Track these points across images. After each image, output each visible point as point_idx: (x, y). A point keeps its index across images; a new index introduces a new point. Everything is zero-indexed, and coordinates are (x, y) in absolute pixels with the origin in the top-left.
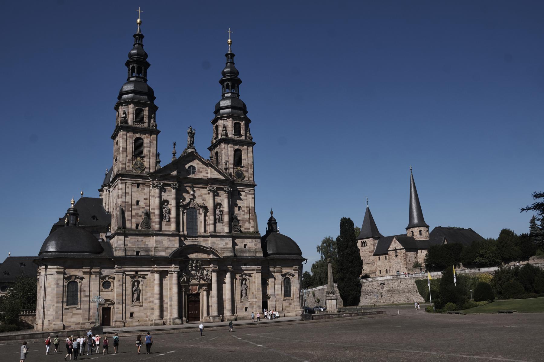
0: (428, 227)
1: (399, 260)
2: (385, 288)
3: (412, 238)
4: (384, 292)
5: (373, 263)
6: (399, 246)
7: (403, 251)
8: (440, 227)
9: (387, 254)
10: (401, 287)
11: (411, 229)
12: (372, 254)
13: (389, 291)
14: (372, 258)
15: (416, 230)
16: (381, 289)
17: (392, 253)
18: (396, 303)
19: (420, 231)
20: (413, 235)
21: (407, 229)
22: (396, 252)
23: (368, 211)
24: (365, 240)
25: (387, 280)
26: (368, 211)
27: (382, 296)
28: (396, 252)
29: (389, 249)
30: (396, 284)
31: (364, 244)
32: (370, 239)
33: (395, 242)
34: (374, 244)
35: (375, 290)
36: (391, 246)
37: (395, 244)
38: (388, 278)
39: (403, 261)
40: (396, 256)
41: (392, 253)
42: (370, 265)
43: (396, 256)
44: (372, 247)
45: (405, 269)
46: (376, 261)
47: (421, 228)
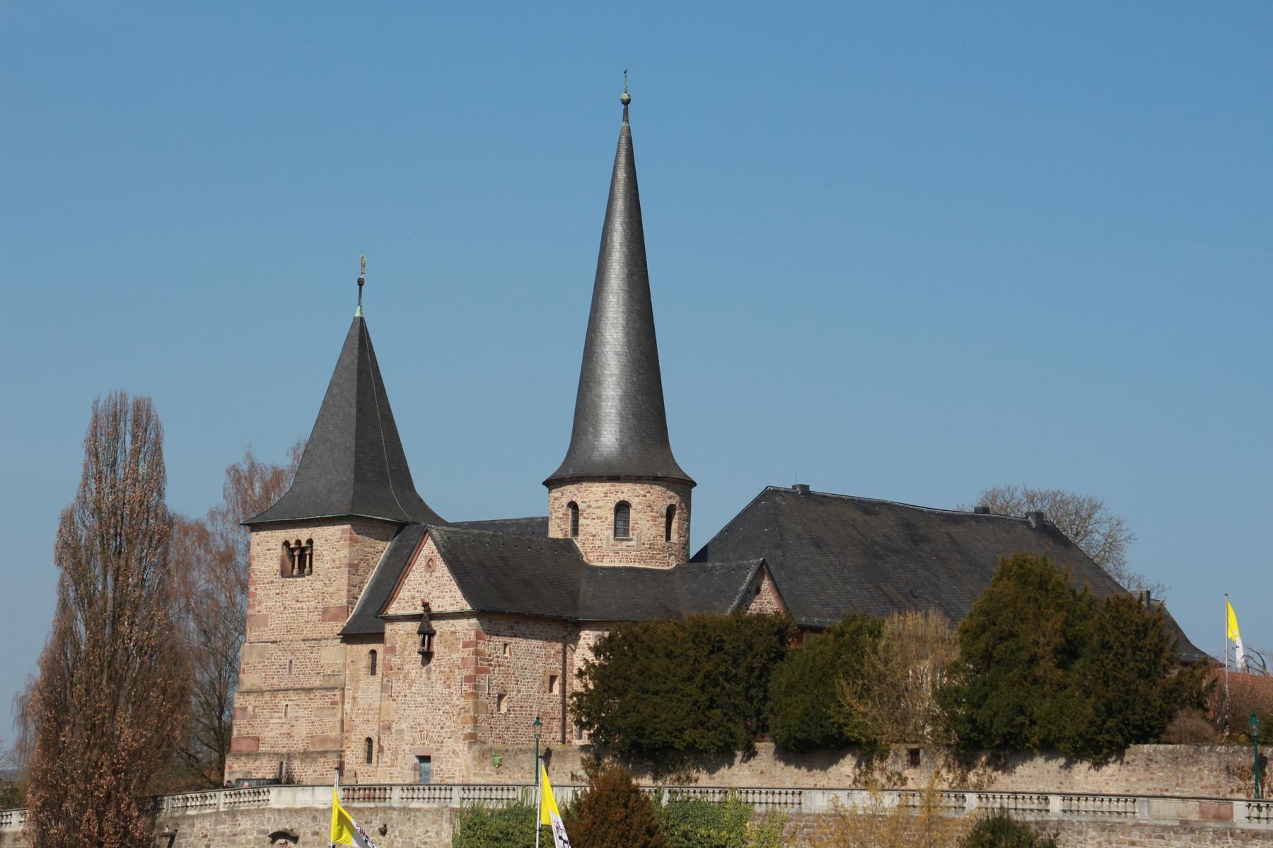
1: (439, 687)
3: (567, 547)
5: (334, 688)
6: (449, 596)
7: (467, 628)
9: (379, 637)
11: (570, 492)
12: (339, 627)
14: (335, 654)
17: (402, 635)
20: (575, 532)
21: (551, 484)
22: (427, 634)
24: (303, 534)
28: (427, 634)
29: (393, 610)
31: (299, 559)
32: (336, 532)
33: (430, 565)
34: (353, 568)
36: (405, 592)
37: (431, 583)
39: (458, 698)
40: (427, 656)
42: (318, 700)
43: (427, 656)
45: (462, 747)
46: (355, 679)
47: (626, 491)
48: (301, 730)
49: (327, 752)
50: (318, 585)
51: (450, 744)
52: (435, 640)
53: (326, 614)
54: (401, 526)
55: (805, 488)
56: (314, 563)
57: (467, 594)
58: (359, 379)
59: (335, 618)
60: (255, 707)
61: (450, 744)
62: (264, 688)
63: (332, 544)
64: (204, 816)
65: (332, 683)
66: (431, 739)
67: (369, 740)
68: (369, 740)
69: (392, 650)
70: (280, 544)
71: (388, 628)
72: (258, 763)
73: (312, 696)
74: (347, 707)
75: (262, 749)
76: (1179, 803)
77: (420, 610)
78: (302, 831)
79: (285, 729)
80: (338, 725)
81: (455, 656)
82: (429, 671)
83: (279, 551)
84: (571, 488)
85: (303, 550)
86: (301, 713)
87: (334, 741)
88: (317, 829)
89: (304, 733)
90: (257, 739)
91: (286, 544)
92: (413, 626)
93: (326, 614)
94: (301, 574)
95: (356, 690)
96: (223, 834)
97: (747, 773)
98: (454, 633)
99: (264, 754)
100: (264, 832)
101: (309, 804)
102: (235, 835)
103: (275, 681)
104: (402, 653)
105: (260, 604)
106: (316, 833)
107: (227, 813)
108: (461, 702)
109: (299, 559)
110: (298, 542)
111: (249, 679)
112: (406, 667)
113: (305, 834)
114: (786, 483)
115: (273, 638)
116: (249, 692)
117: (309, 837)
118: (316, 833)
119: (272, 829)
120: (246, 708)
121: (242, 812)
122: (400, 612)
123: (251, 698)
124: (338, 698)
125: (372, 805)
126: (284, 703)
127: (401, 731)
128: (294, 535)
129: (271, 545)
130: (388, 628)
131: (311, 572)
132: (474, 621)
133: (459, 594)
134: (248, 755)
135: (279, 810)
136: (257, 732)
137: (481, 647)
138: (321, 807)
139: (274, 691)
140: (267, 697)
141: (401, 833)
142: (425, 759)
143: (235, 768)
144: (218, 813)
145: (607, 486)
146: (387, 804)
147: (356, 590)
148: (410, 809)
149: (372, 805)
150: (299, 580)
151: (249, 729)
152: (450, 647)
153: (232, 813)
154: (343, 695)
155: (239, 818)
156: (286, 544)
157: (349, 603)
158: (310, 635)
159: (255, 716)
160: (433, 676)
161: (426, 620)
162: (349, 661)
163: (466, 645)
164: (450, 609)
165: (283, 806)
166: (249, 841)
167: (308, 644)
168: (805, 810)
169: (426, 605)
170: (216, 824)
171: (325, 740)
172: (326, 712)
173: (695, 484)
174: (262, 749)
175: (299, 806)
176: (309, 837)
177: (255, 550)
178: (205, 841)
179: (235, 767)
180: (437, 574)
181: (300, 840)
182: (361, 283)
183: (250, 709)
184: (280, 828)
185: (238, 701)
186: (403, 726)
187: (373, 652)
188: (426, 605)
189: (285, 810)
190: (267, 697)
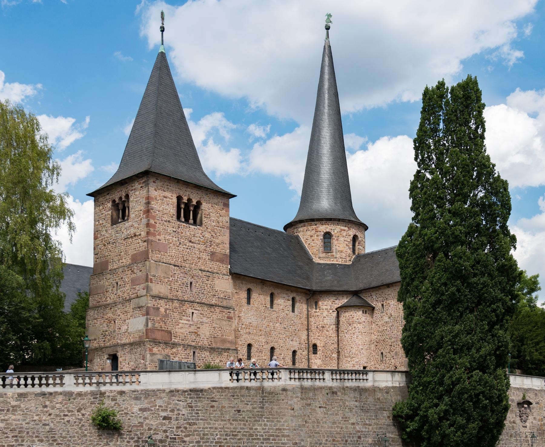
42: (217, 313)
48: (206, 331)
49: (229, 349)
50: (208, 235)
60: (166, 310)
62: (170, 296)
65: (225, 303)
67: (250, 346)
73: (212, 310)
79: (193, 329)
86: (205, 320)
87: (231, 342)
89: (208, 334)
90: (170, 333)
95: (240, 312)
99: (180, 345)
103: (179, 293)
120: (158, 309)
123: (162, 302)
126: (191, 311)
134: (166, 343)
139: (182, 302)
150: (193, 227)
159: (166, 316)
167: (204, 273)
171: (224, 341)
172: (224, 323)
179: (155, 350)
183: (162, 310)
190: (176, 304)
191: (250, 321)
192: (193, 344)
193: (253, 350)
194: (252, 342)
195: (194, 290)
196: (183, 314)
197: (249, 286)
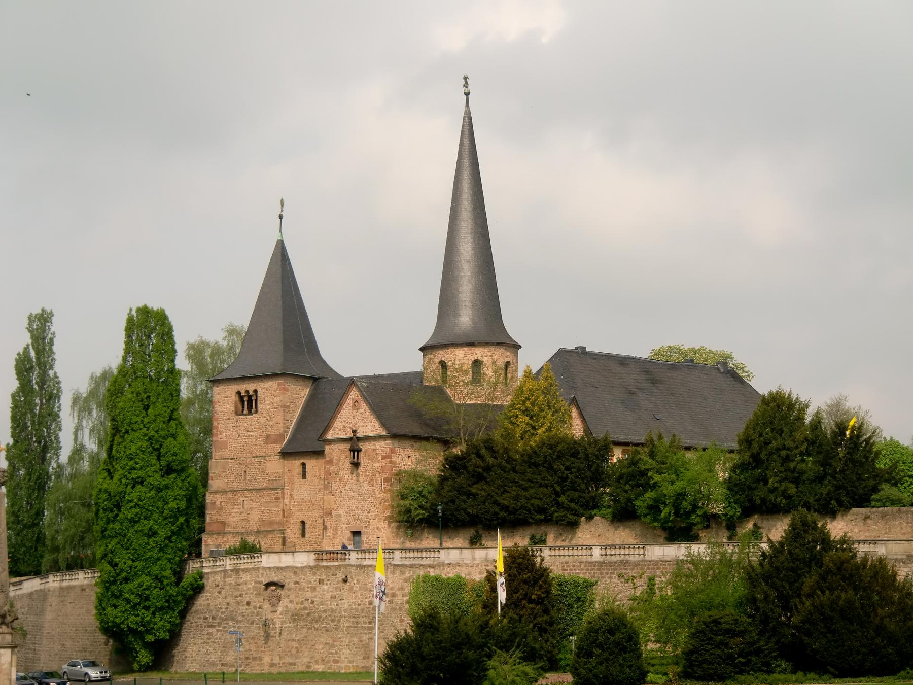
0: (517, 347)
1: (365, 486)
2: (285, 602)
4: (277, 620)
5: (276, 489)
6: (370, 426)
8: (581, 352)
9: (319, 453)
10: (345, 605)
12: (278, 448)
13: (296, 617)
14: (275, 466)
15: (460, 357)
16: (266, 606)
17: (337, 453)
18: (320, 668)
19: (477, 364)
22: (355, 451)
23: (281, 256)
24: (251, 387)
25: (294, 570)
26: (281, 256)
27: (267, 637)
28: (355, 451)
29: (330, 435)
30: (326, 589)
31: (248, 403)
32: (272, 384)
34: (286, 408)
35: (243, 608)
36: (338, 424)
37: (355, 418)
38: (303, 559)
40: (356, 465)
41: (337, 453)
43: (356, 465)
44: (279, 418)
46: (291, 482)
47: (478, 353)
48: (255, 517)
51: (375, 523)
52: (361, 455)
53: (268, 439)
54: (315, 379)
55: (583, 348)
56: (259, 405)
57: (383, 425)
58: (283, 283)
59: (276, 442)
61: (375, 523)
63: (269, 393)
64: (215, 573)
66: (361, 520)
67: (303, 523)
68: (303, 523)
69: (331, 462)
70: (234, 393)
71: (327, 448)
72: (225, 539)
74: (287, 501)
75: (227, 529)
76: (906, 544)
77: (350, 435)
78: (287, 581)
79: (243, 516)
80: (281, 513)
81: (376, 465)
82: (358, 476)
83: (234, 398)
84: (441, 352)
85: (250, 397)
86: (254, 505)
87: (279, 523)
88: (297, 579)
89: (257, 519)
90: (224, 523)
91: (239, 393)
92: (346, 447)
93: (268, 439)
94: (250, 413)
95: (292, 489)
96: (230, 584)
97: (588, 536)
98: (374, 450)
100: (260, 583)
101: (291, 564)
102: (239, 585)
104: (337, 464)
105: (221, 433)
106: (297, 583)
107: (232, 570)
108: (382, 496)
109: (248, 403)
110: (247, 392)
111: (215, 483)
112: (341, 473)
113: (289, 582)
114: (571, 346)
115: (232, 456)
116: (216, 492)
117: (292, 585)
118: (297, 583)
119: (265, 580)
121: (243, 570)
122: (335, 437)
123: (218, 496)
124: (280, 495)
125: (336, 563)
127: (339, 515)
128: (244, 387)
129: (228, 394)
130: (327, 448)
131: (256, 412)
132: (389, 442)
133: (377, 425)
134: (218, 534)
135: (270, 568)
136: (224, 518)
137: (394, 459)
138: (299, 565)
139: (235, 491)
140: (229, 495)
141: (358, 581)
142: (357, 534)
143: (209, 542)
144: (225, 571)
145: (466, 349)
146: (347, 562)
147: (288, 424)
148: (364, 566)
149: (336, 563)
151: (218, 516)
152: (373, 459)
153: (236, 571)
154: (283, 493)
155: (241, 573)
156: (239, 393)
157: (285, 432)
158: (257, 454)
159: (221, 508)
160: (361, 479)
161: (355, 444)
162: (286, 470)
163: (384, 457)
164: (372, 434)
165: (271, 565)
166: (249, 589)
168: (647, 558)
169: (354, 432)
170: (224, 577)
171: (271, 523)
173: (519, 347)
174: (227, 529)
175: (283, 565)
176: (292, 585)
177: (216, 398)
178: (218, 589)
179: (209, 542)
180: (362, 411)
181: (286, 586)
182: (281, 217)
183: (218, 503)
184: (271, 580)
185: (209, 498)
186: (341, 512)
187: (304, 465)
188: (354, 432)
189: (274, 568)
190: (229, 495)
191: (302, 497)
192: (244, 530)
193: (307, 526)
194: (304, 519)
195: (248, 478)
196: (235, 503)
197: (302, 461)
